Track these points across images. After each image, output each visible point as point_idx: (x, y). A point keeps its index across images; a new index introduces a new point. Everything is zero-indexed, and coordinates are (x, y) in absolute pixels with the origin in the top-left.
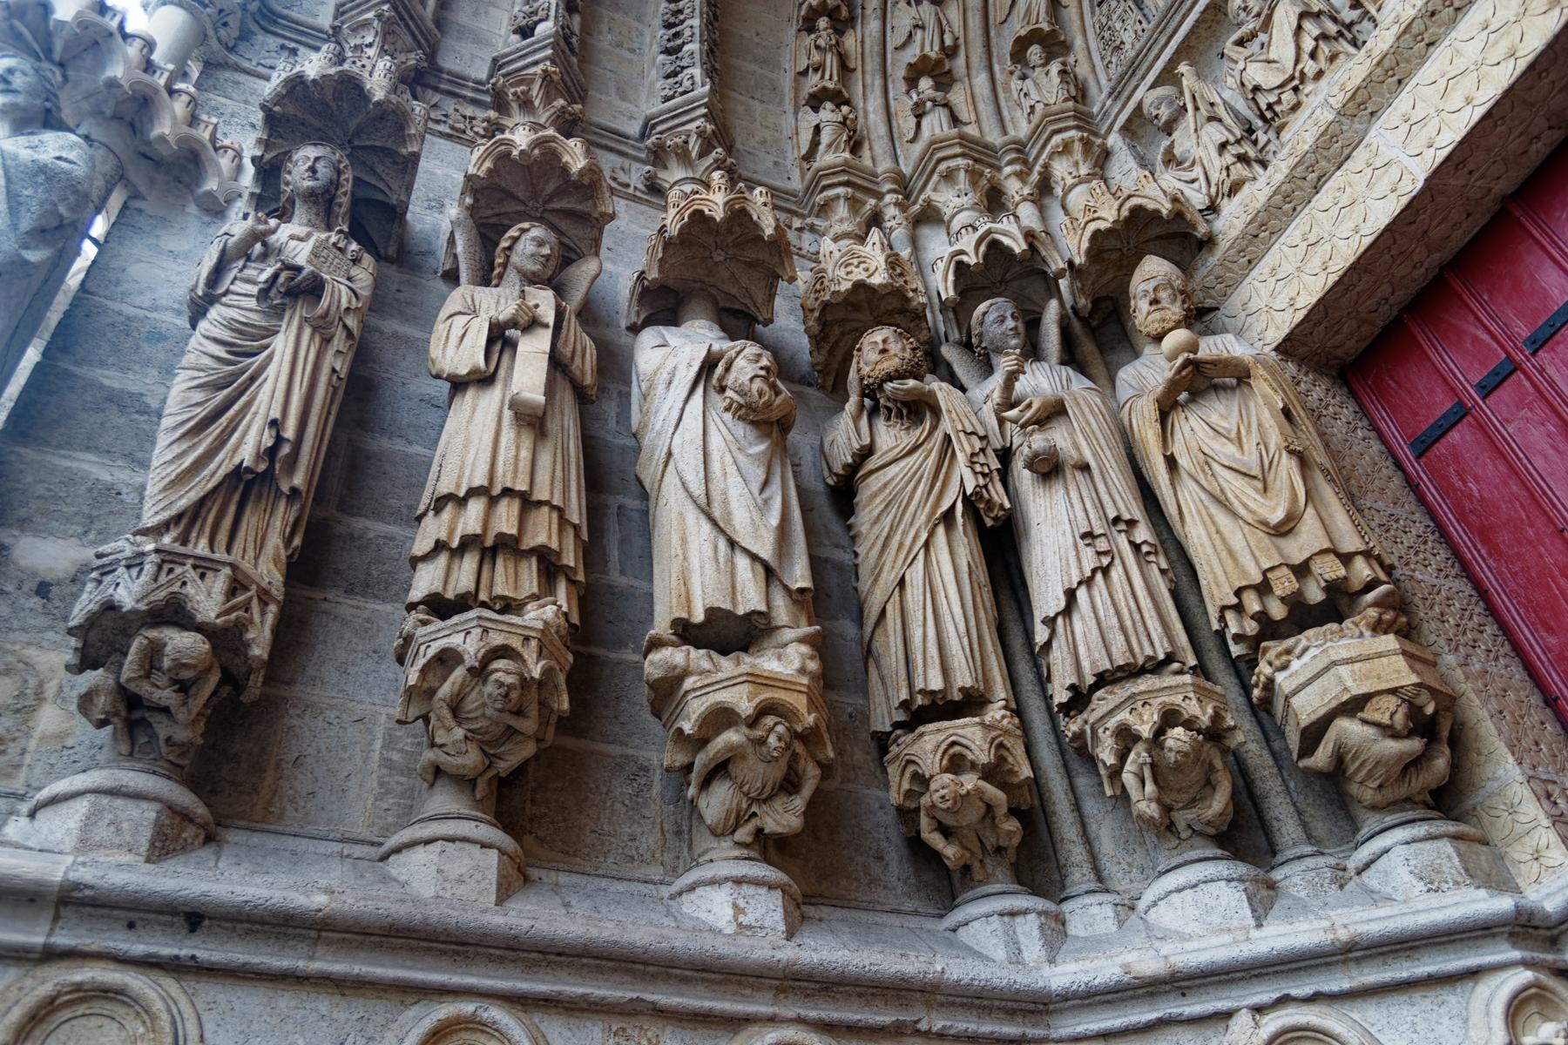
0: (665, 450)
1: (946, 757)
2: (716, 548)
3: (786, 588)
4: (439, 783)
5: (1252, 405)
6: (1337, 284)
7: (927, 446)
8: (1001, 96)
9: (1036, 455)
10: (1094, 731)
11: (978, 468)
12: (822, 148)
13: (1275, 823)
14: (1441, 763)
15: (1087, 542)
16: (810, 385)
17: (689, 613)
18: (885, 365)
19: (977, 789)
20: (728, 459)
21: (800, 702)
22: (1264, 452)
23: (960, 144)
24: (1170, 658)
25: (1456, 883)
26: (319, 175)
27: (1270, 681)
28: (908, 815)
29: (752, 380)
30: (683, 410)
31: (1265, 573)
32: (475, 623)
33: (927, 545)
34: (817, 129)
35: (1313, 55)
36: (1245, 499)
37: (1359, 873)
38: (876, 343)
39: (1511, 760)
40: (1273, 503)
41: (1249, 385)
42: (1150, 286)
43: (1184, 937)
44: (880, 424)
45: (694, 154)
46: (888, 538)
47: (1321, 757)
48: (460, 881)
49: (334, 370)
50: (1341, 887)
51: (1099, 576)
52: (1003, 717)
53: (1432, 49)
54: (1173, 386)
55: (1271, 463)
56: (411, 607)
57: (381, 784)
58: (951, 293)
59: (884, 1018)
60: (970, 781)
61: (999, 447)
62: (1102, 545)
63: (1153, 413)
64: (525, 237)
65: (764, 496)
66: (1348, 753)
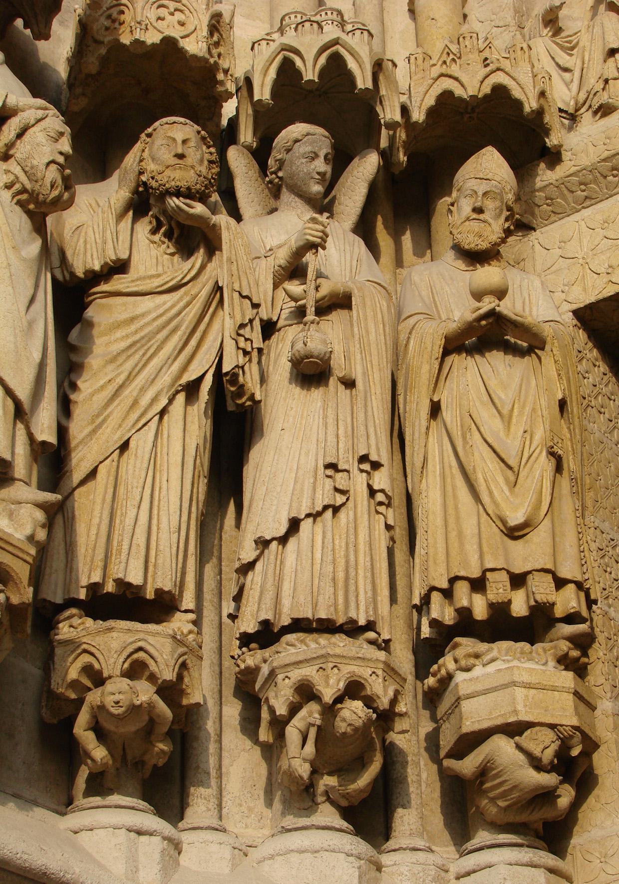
1: (129, 661)
3: (31, 436)
10: (272, 674)
15: (330, 472)
18: (177, 174)
19: (151, 706)
22: (528, 443)
27: (450, 677)
33: (163, 413)
36: (493, 488)
37: (458, 878)
38: (174, 140)
42: (482, 188)
47: (468, 765)
51: (329, 513)
52: (190, 632)
61: (265, 318)
62: (341, 480)
63: (436, 348)
66: (493, 769)
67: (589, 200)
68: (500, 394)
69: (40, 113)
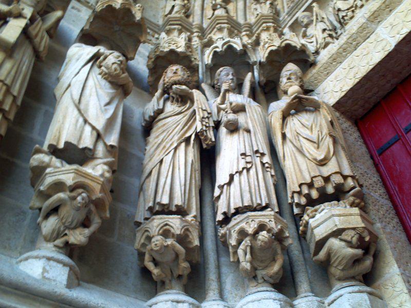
2: (77, 121)
3: (105, 144)
5: (319, 118)
7: (185, 113)
9: (229, 121)
11: (204, 123)
13: (299, 283)
15: (243, 157)
19: (172, 244)
20: (94, 90)
22: (320, 135)
27: (307, 223)
28: (141, 255)
29: (113, 64)
30: (80, 69)
31: (312, 178)
33: (176, 149)
34: (173, 7)
37: (329, 305)
39: (396, 265)
40: (320, 153)
41: (319, 111)
42: (288, 73)
47: (322, 254)
51: (245, 171)
52: (192, 220)
55: (322, 139)
58: (210, 62)
60: (170, 242)
61: (215, 120)
62: (248, 159)
65: (106, 107)
67: (328, 74)
68: (306, 123)
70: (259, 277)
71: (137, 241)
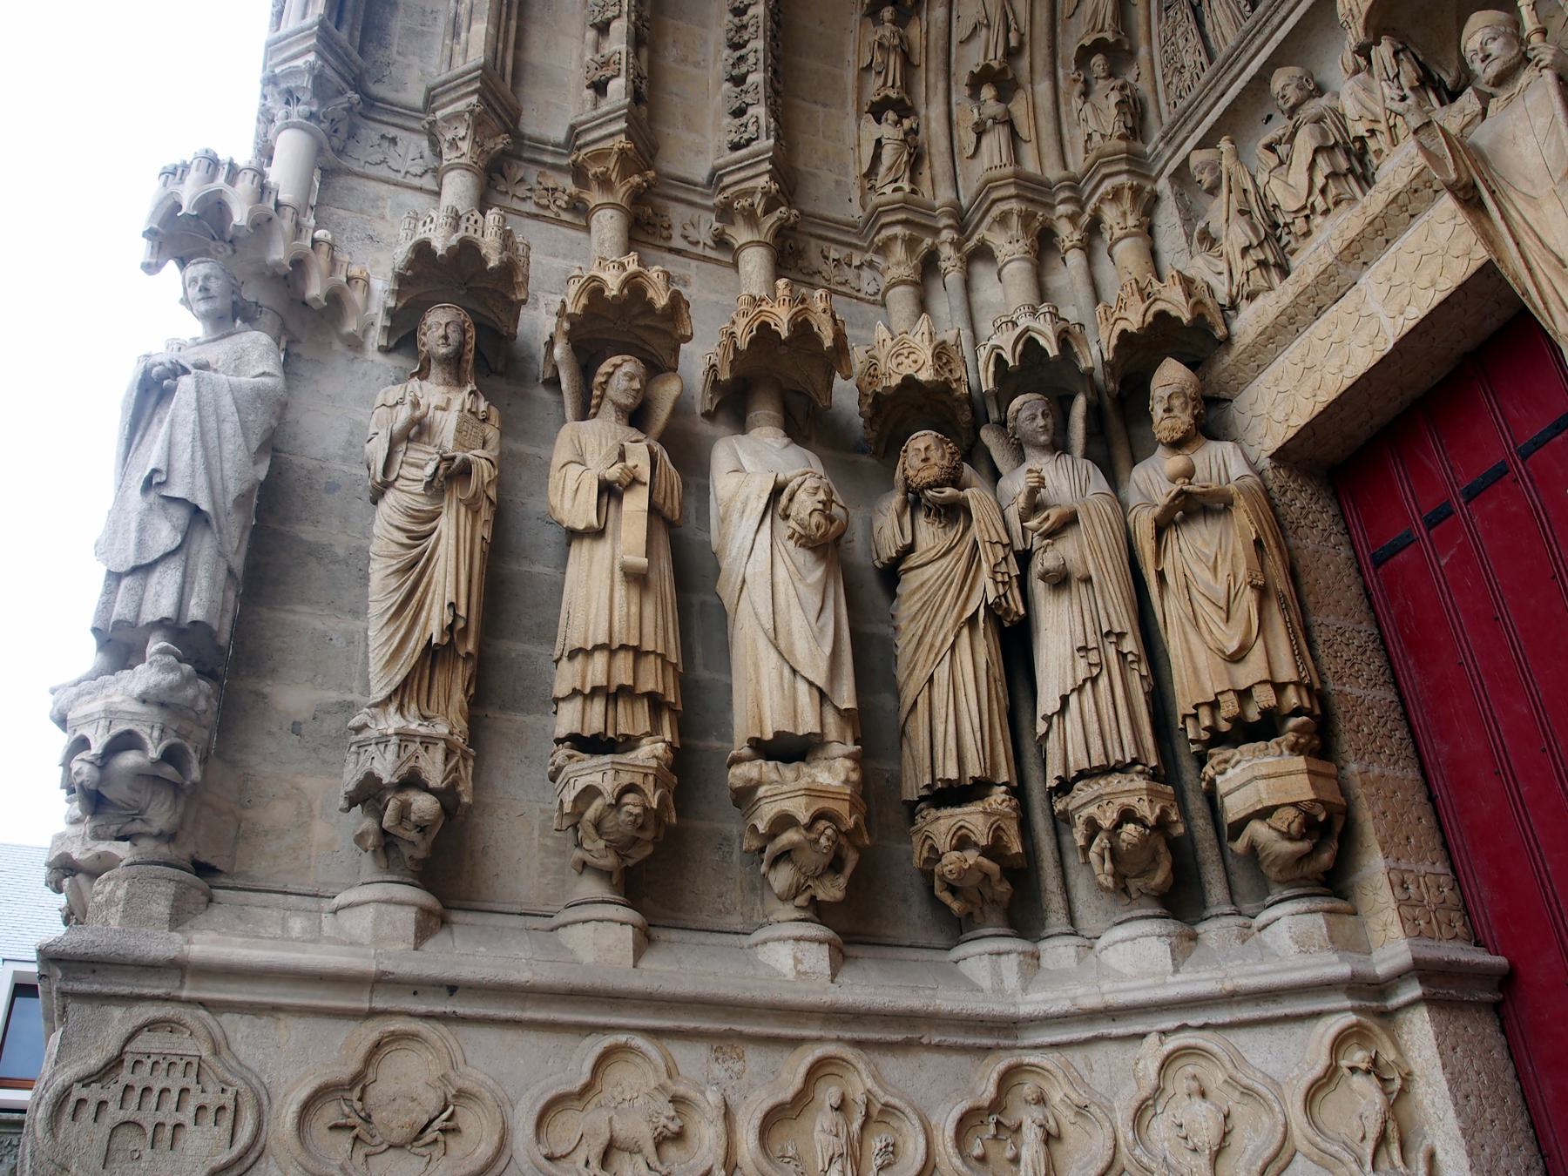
0: (740, 578)
3: (836, 708)
4: (586, 871)
5: (1231, 532)
6: (1321, 413)
7: (959, 549)
8: (1063, 109)
9: (1047, 572)
11: (999, 578)
12: (882, 170)
14: (1326, 857)
16: (864, 452)
17: (761, 732)
19: (978, 865)
21: (843, 808)
23: (1015, 183)
24: (1135, 762)
25: (1321, 947)
26: (450, 341)
28: (928, 875)
29: (810, 514)
31: (1216, 695)
32: (609, 766)
35: (1323, 191)
37: (1259, 931)
39: (1380, 855)
42: (1166, 392)
43: (1122, 977)
44: (921, 519)
45: (759, 211)
46: (921, 637)
47: (1240, 845)
48: (609, 950)
49: (483, 538)
50: (1244, 941)
51: (1088, 685)
52: (1003, 801)
53: (1413, 220)
54: (1169, 510)
56: (559, 741)
57: (542, 864)
58: (991, 385)
59: (898, 1037)
60: (972, 857)
64: (619, 373)
65: (819, 624)
67: (1260, 368)
69: (799, 480)
70: (1132, 889)
71: (917, 854)
